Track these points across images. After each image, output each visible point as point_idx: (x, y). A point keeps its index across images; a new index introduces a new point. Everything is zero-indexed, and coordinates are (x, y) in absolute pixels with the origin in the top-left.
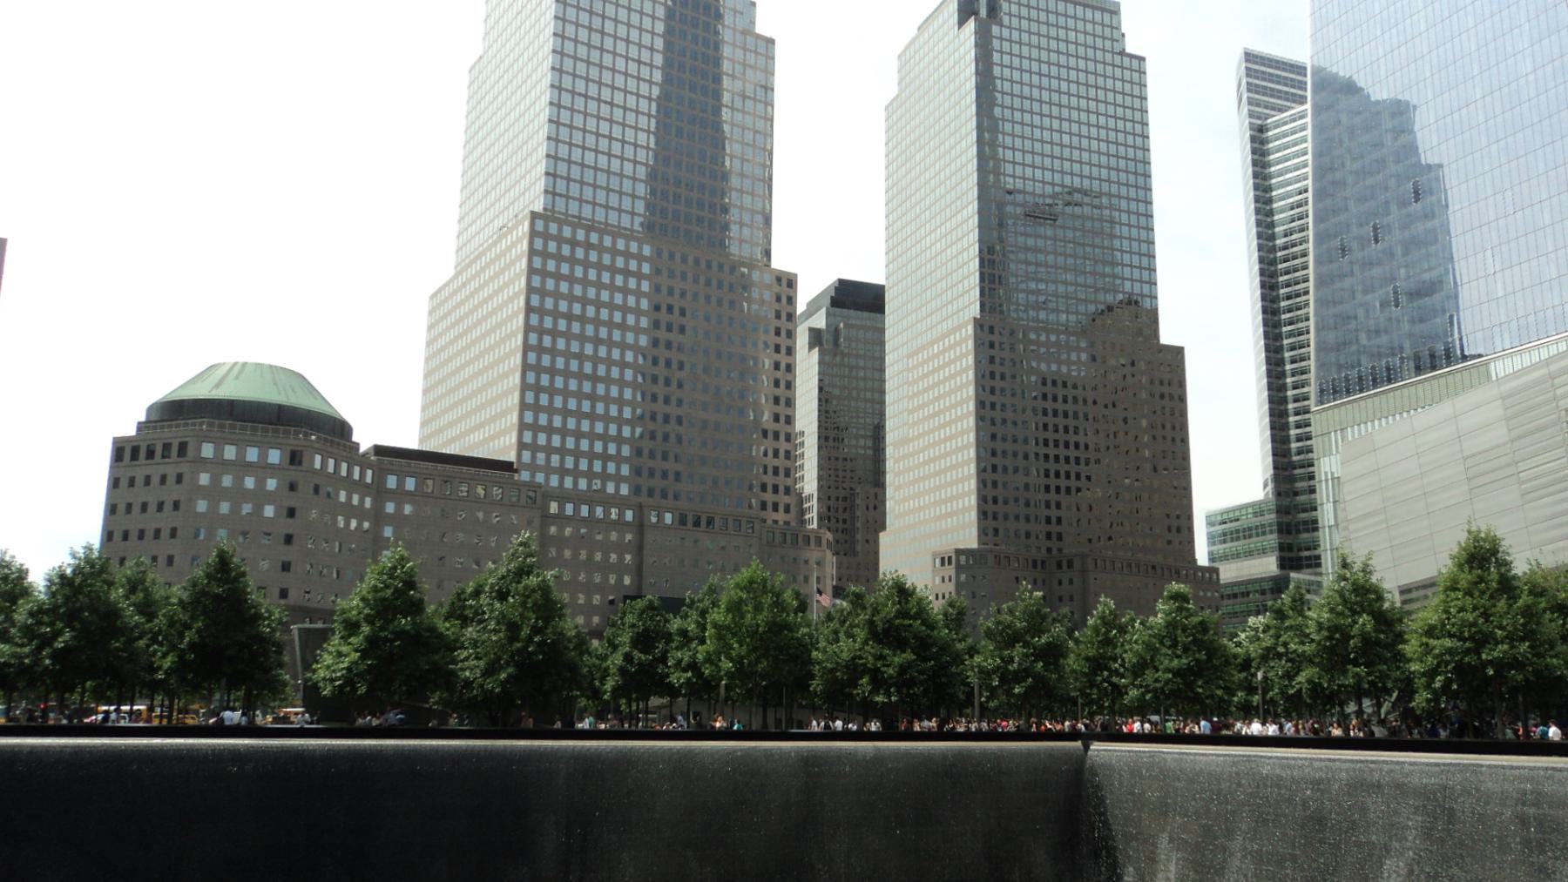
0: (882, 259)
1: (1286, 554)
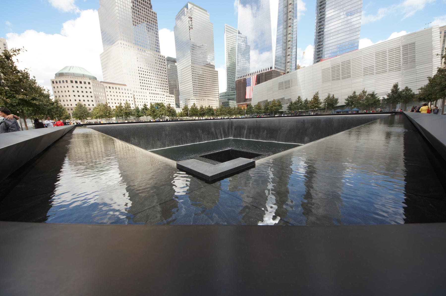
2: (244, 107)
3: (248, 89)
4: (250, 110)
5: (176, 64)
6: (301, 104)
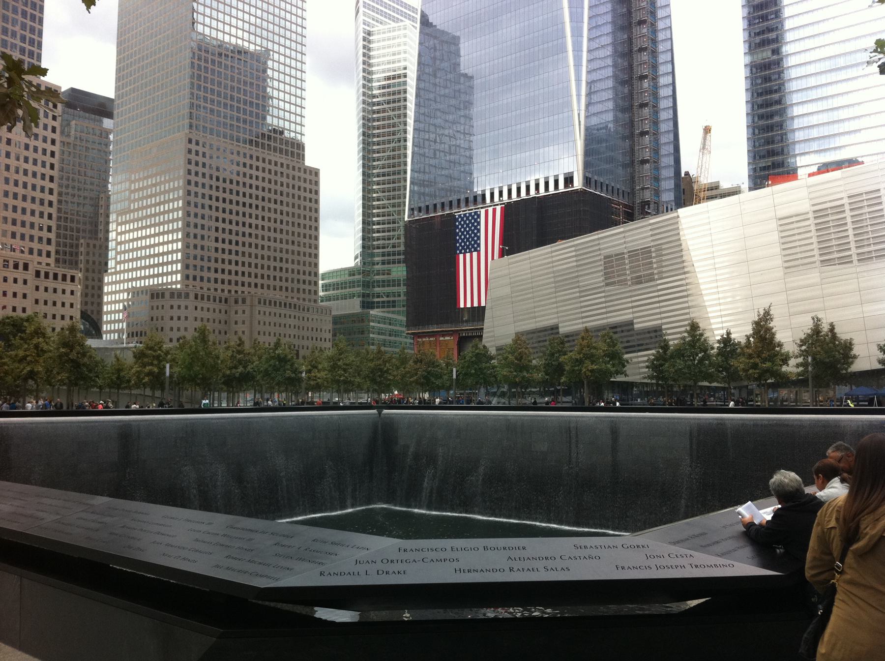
1: (366, 299)
2: (443, 349)
3: (465, 263)
4: (478, 376)
5: (107, 123)
6: (707, 357)
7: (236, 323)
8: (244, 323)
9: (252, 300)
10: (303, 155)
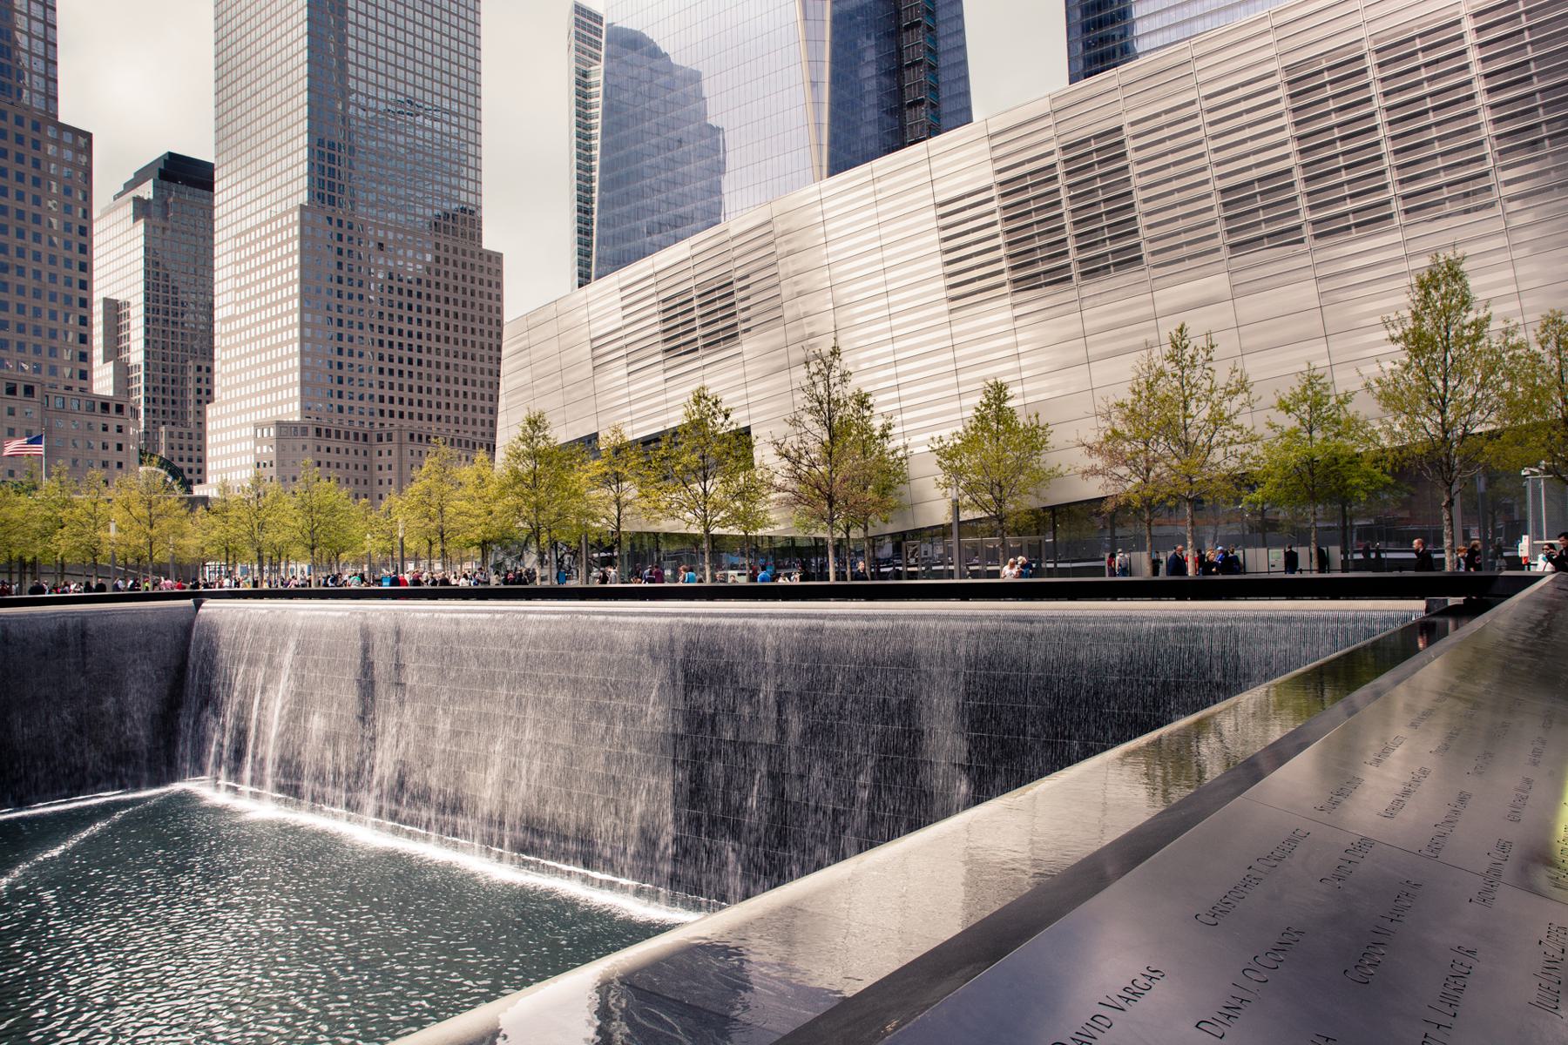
0: (211, 137)
7: (380, 468)
8: (390, 467)
9: (401, 436)
10: (480, 235)
